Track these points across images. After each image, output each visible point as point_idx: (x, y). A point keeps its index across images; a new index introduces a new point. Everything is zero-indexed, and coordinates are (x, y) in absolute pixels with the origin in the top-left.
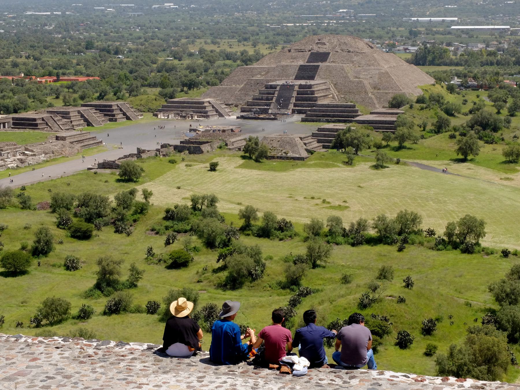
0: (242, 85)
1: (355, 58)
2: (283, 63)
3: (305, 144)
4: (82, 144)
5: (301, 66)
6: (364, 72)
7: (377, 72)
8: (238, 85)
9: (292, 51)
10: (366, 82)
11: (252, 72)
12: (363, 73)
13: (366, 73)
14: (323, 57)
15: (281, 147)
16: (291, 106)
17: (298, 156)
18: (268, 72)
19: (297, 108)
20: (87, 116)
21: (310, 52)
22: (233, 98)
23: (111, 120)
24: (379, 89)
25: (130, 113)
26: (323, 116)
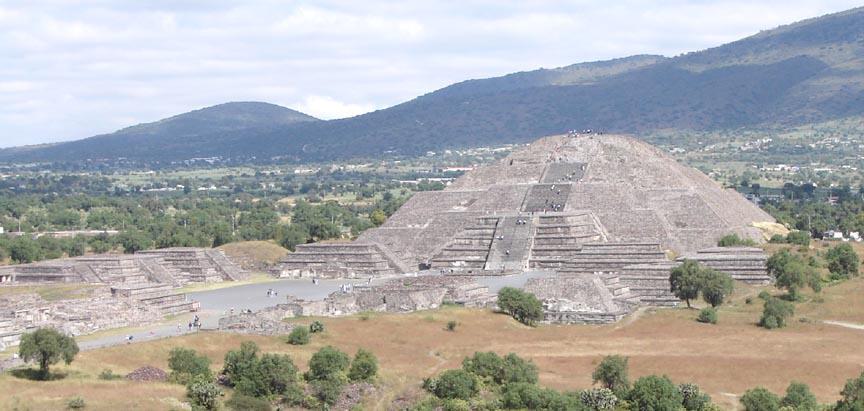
0: (426, 225)
1: (635, 172)
2: (500, 183)
3: (612, 291)
4: (161, 307)
5: (536, 186)
6: (654, 195)
7: (679, 195)
8: (417, 226)
9: (514, 162)
10: (661, 214)
11: (443, 200)
12: (653, 198)
13: (657, 198)
14: (578, 170)
15: (567, 296)
16: (530, 258)
17: (600, 311)
18: (472, 201)
19: (538, 258)
20: (153, 269)
21: (549, 164)
22: (410, 248)
23: (192, 278)
24: (684, 226)
25: (228, 268)
26: (599, 265)
